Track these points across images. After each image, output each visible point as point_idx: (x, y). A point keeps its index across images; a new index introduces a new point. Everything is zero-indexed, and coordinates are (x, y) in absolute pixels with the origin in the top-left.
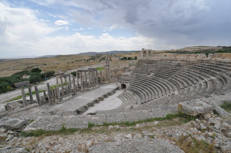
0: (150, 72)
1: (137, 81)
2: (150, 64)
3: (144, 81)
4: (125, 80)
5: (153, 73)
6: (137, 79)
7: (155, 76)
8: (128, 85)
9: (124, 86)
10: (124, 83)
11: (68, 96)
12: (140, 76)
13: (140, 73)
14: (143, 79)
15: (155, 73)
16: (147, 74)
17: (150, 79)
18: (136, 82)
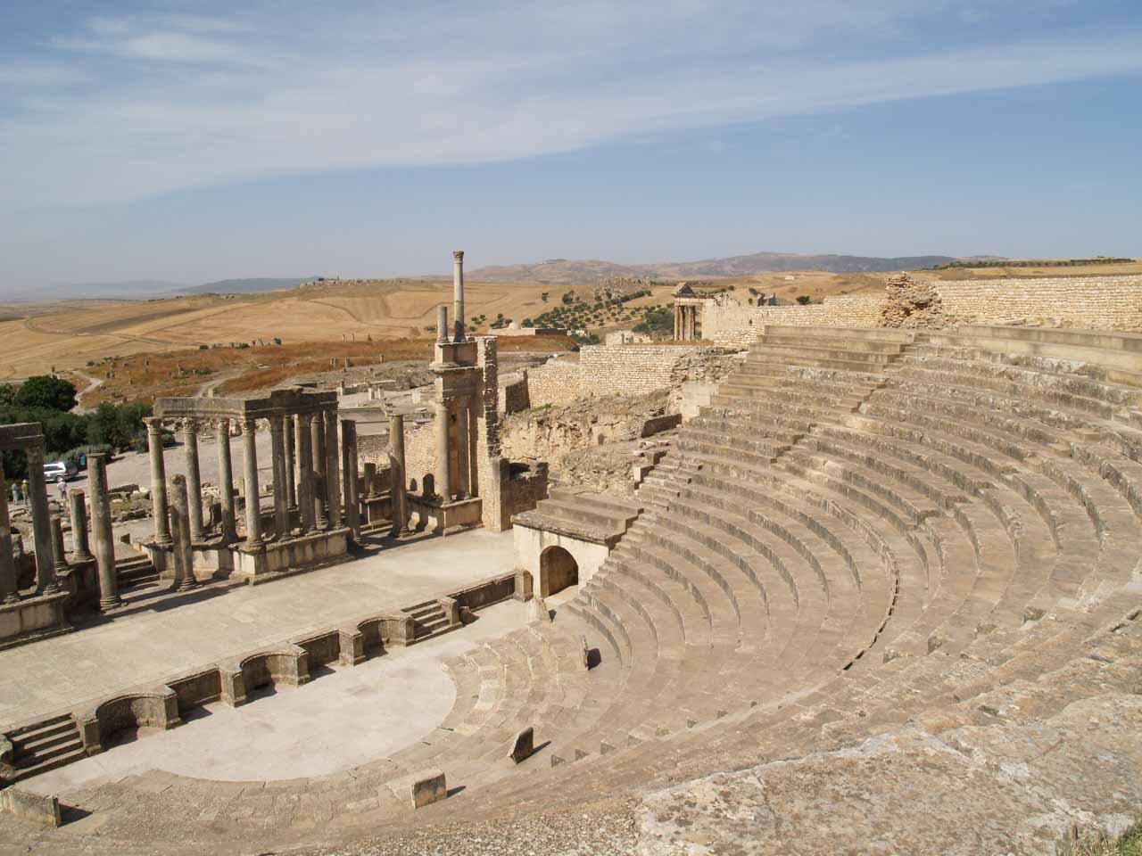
0: (822, 448)
1: (677, 528)
2: (846, 366)
3: (731, 529)
4: (579, 515)
5: (830, 463)
6: (686, 511)
7: (842, 489)
8: (590, 558)
9: (560, 570)
10: (566, 543)
11: (15, 615)
12: (720, 485)
13: (730, 454)
14: (735, 508)
15: (852, 457)
16: (791, 469)
17: (786, 522)
18: (663, 543)
